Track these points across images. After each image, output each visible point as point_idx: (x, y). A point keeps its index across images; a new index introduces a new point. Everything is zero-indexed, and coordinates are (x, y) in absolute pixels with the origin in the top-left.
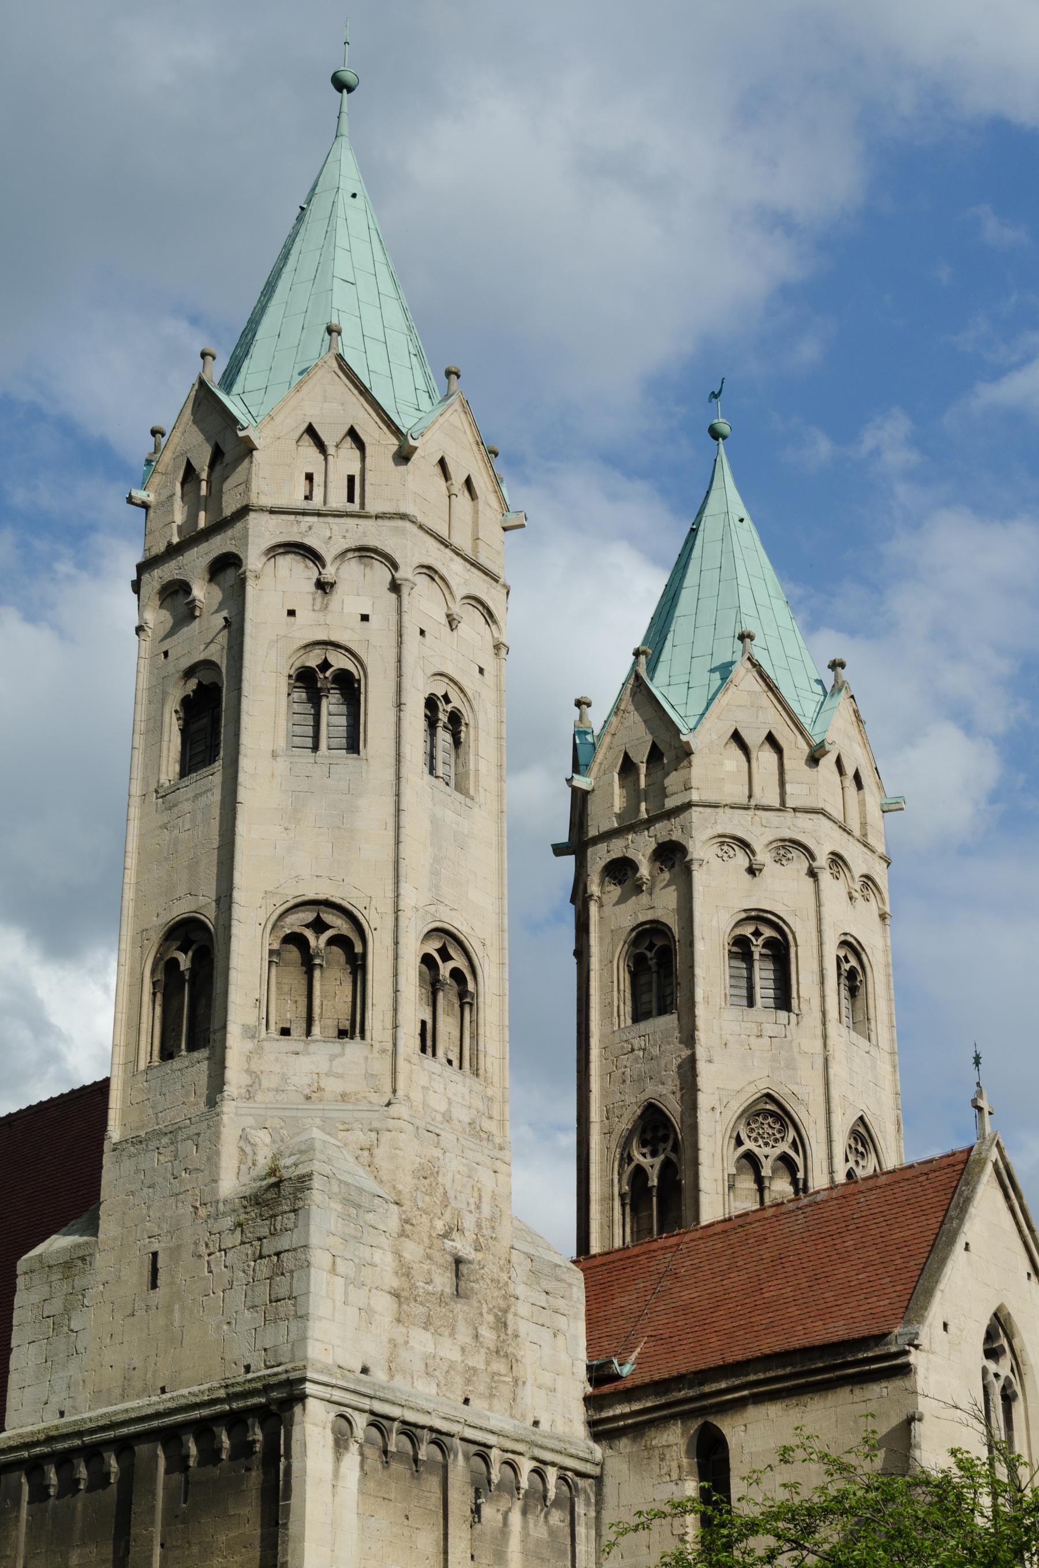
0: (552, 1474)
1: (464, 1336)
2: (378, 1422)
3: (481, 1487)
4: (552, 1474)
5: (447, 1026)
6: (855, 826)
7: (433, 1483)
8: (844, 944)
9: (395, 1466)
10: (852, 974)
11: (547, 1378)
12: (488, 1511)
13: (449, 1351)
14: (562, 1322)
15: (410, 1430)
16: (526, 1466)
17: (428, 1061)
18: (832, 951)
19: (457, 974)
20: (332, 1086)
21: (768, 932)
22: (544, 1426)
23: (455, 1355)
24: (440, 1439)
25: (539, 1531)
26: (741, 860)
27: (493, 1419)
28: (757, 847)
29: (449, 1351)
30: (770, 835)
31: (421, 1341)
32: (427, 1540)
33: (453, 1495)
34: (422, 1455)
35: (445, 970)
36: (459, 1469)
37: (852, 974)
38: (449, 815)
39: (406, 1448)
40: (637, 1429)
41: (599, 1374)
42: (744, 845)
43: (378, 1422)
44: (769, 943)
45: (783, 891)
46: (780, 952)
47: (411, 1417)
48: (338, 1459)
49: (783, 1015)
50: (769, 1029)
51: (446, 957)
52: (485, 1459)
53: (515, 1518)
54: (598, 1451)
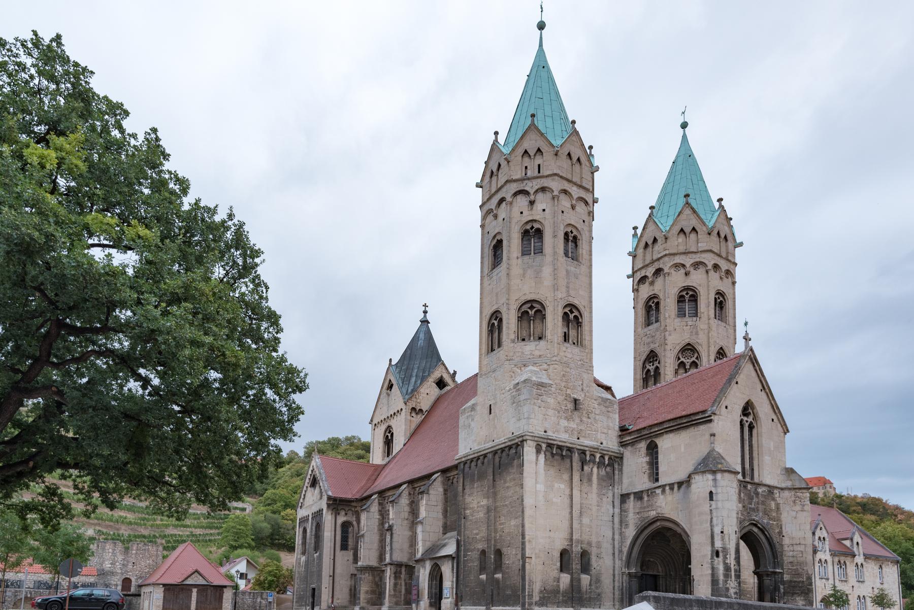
0: (607, 458)
1: (577, 420)
2: (550, 446)
3: (583, 463)
4: (607, 458)
5: (573, 333)
6: (724, 255)
7: (568, 461)
8: (717, 293)
9: (556, 457)
10: (721, 302)
11: (605, 431)
12: (586, 468)
13: (573, 425)
14: (611, 415)
15: (560, 447)
16: (598, 456)
17: (566, 344)
18: (712, 296)
19: (575, 317)
20: (537, 353)
21: (691, 293)
22: (604, 444)
23: (575, 426)
24: (570, 450)
25: (603, 472)
26: (682, 271)
27: (587, 442)
28: (688, 266)
29: (573, 425)
30: (692, 261)
31: (564, 423)
32: (566, 476)
33: (574, 464)
34: (564, 453)
35: (571, 316)
36: (576, 457)
37: (721, 302)
38: (573, 269)
39: (558, 453)
40: (633, 443)
41: (623, 429)
42: (683, 266)
43: (550, 446)
44: (692, 296)
45: (697, 279)
46: (694, 299)
47: (560, 444)
48: (537, 457)
49: (695, 319)
50: (690, 323)
51: (572, 312)
52: (585, 454)
53: (595, 470)
54: (621, 449)
